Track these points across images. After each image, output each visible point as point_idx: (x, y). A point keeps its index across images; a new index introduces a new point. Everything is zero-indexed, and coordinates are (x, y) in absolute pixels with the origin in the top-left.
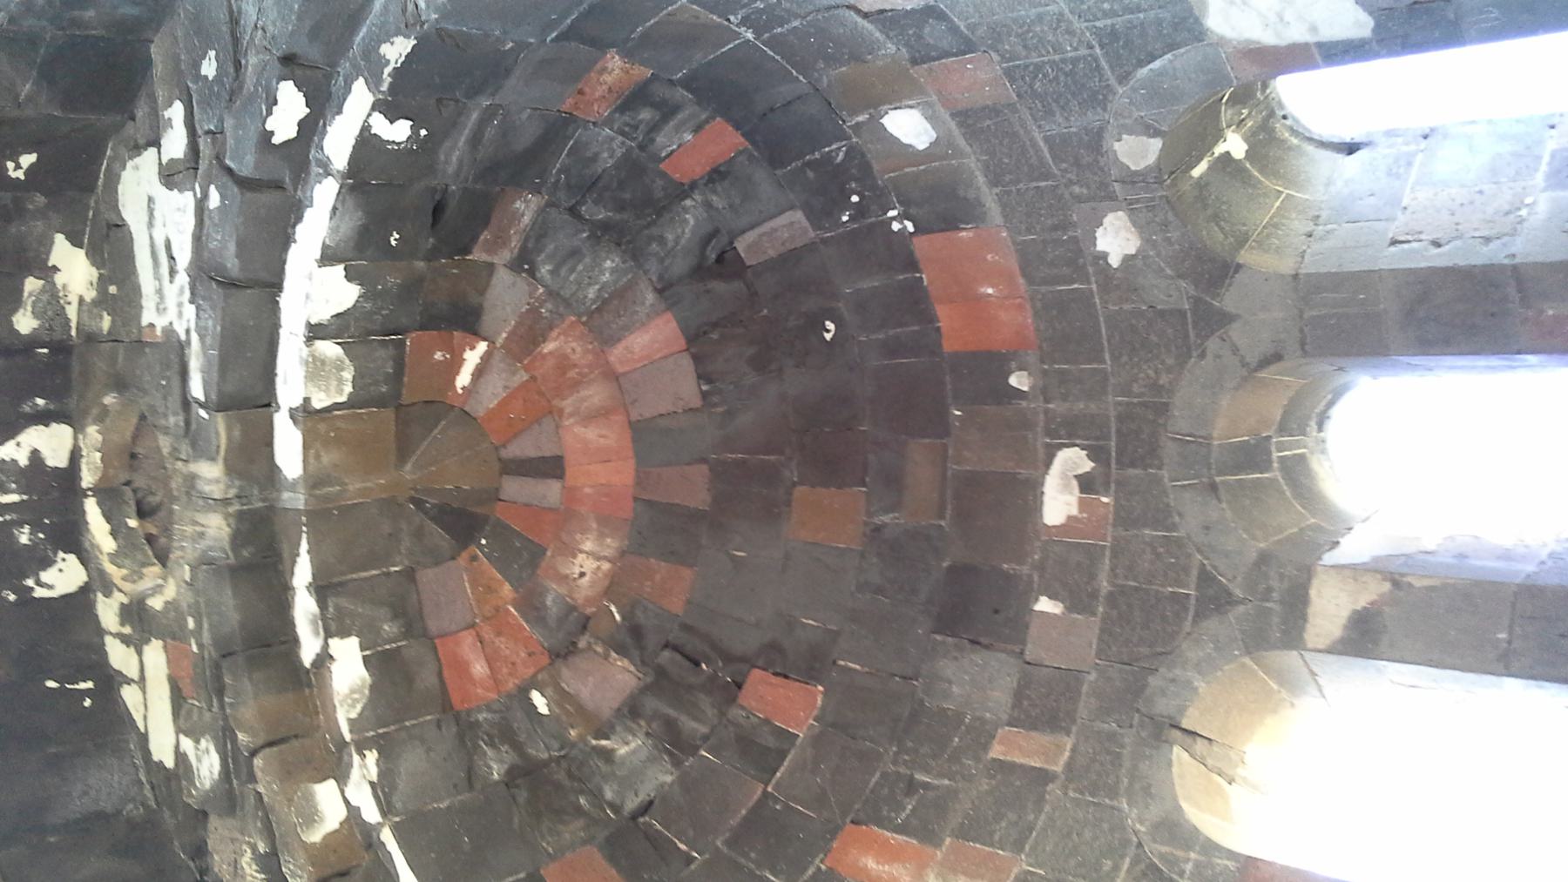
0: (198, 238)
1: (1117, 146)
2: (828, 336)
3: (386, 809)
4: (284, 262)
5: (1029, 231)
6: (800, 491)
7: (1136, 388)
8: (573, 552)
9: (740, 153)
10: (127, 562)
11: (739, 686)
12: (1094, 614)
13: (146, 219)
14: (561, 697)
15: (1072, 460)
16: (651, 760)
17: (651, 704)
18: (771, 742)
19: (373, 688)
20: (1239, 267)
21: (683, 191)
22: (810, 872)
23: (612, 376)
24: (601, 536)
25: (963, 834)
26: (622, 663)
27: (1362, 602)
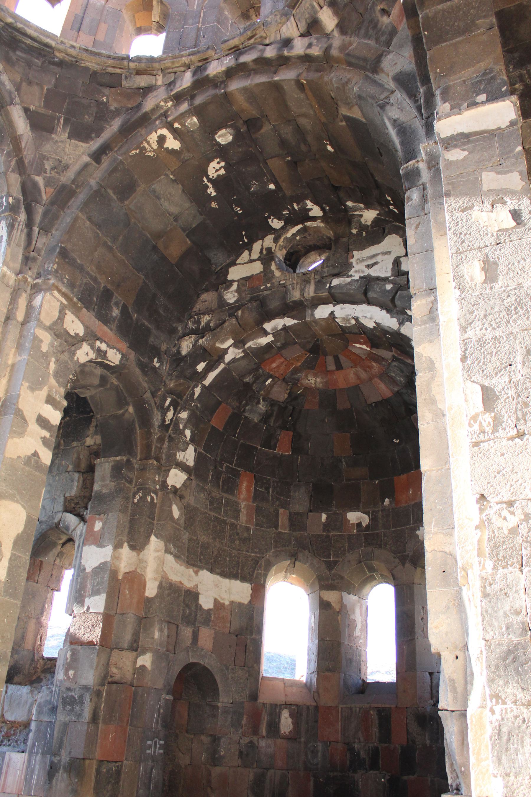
0: (378, 279)
2: (394, 440)
3: (229, 363)
4: (376, 305)
6: (349, 435)
7: (386, 538)
8: (315, 376)
10: (285, 243)
11: (287, 430)
12: (323, 532)
14: (271, 386)
15: (365, 520)
16: (260, 414)
17: (276, 408)
18: (272, 443)
22: (239, 469)
23: (370, 379)
24: (321, 382)
25: (258, 508)
26: (286, 396)
27: (333, 604)
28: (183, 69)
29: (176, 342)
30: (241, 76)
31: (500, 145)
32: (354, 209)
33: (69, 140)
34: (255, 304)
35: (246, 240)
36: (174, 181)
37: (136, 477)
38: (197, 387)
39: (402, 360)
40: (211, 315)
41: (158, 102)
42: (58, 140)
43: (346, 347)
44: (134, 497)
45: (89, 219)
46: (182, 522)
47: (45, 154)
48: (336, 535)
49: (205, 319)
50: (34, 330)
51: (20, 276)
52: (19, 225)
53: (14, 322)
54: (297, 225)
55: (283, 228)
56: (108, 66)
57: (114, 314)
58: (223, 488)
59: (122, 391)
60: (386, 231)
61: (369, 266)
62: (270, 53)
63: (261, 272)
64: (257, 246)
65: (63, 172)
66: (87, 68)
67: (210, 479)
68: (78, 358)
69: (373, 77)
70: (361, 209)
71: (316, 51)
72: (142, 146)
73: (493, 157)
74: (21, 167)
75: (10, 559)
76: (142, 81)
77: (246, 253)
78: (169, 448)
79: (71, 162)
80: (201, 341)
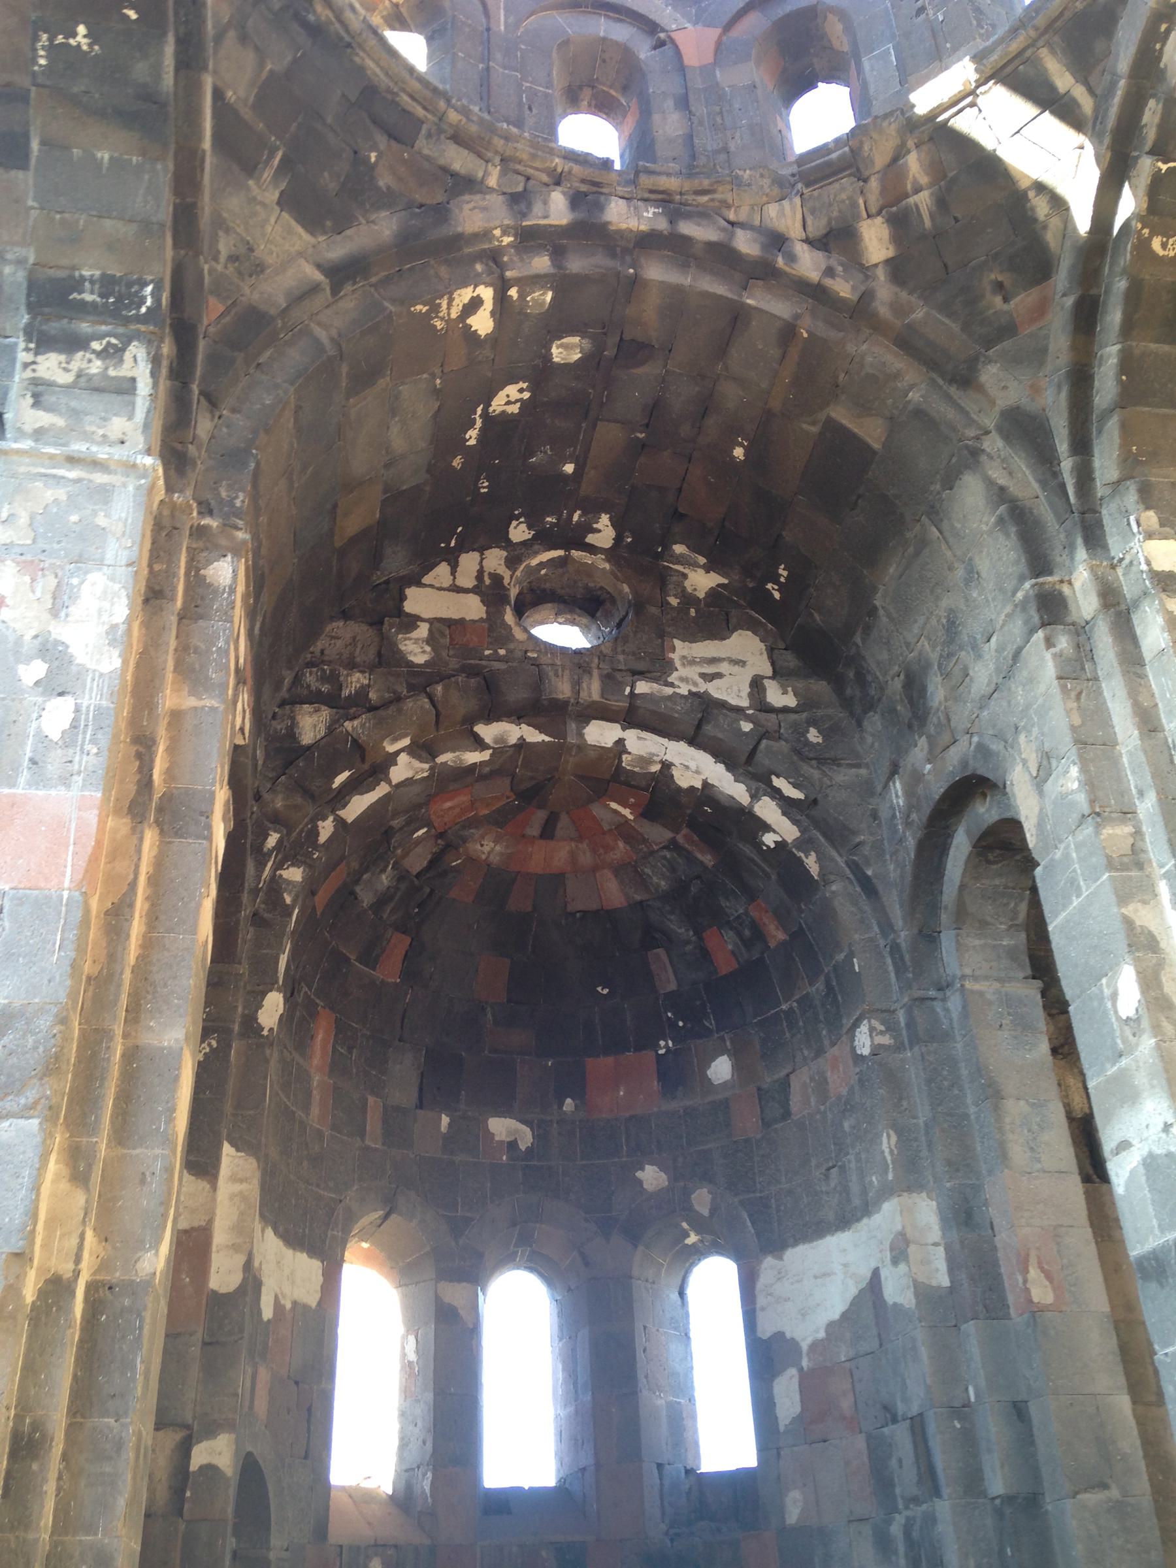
0: (723, 705)
1: (705, 1190)
2: (599, 989)
4: (705, 751)
8: (496, 842)
15: (526, 1137)
17: (403, 886)
20: (636, 1247)
21: (698, 932)
22: (318, 1001)
23: (595, 869)
24: (501, 854)
28: (545, 178)
30: (668, 256)
32: (680, 560)
33: (277, 209)
34: (473, 681)
36: (437, 392)
38: (324, 819)
39: (688, 851)
41: (492, 225)
43: (591, 801)
54: (556, 549)
56: (404, 90)
60: (733, 621)
61: (709, 678)
62: (746, 244)
63: (481, 620)
64: (469, 562)
65: (251, 276)
66: (362, 69)
70: (694, 565)
71: (843, 288)
76: (459, 160)
77: (443, 569)
79: (270, 261)
80: (348, 725)
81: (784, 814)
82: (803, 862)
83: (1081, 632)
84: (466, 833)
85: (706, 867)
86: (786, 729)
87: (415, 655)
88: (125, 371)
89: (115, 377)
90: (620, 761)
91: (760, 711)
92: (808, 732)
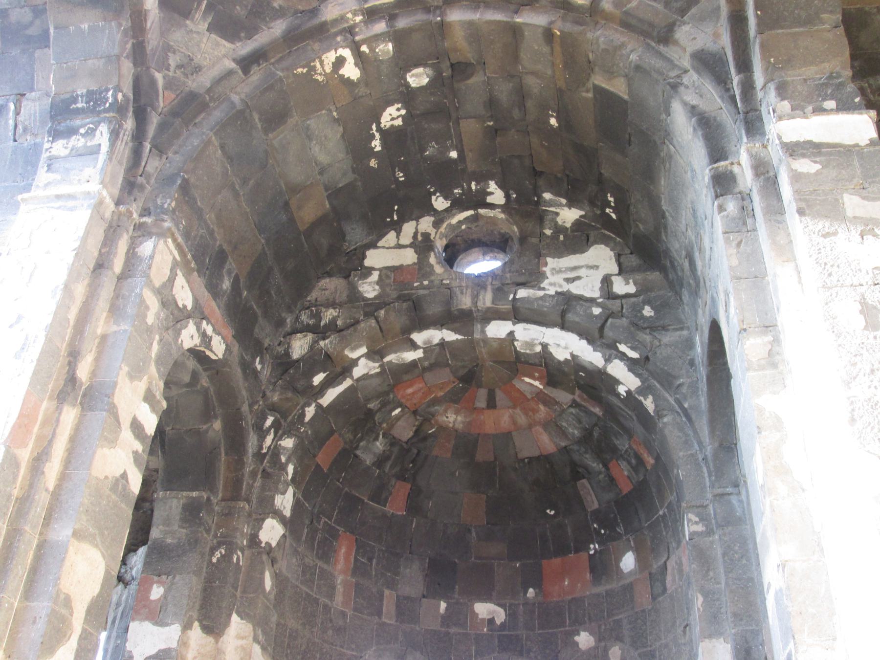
0: (580, 298)
1: (617, 647)
2: (548, 511)
3: (358, 380)
4: (572, 332)
5: (589, 604)
6: (484, 497)
8: (457, 413)
9: (620, 490)
10: (447, 230)
12: (441, 626)
13: (590, 264)
14: (398, 418)
15: (500, 615)
16: (375, 454)
17: (396, 450)
18: (383, 496)
19: (404, 364)
21: (606, 465)
22: (338, 528)
23: (530, 426)
24: (463, 423)
26: (411, 434)
29: (282, 339)
30: (466, 5)
31: (861, 165)
32: (550, 203)
34: (405, 305)
35: (395, 218)
36: (336, 121)
37: (217, 524)
38: (309, 405)
39: (584, 407)
40: (337, 310)
41: (344, 11)
42: (194, 30)
43: (511, 379)
44: (212, 554)
45: (222, 147)
46: (272, 597)
47: (172, 44)
48: (459, 634)
49: (329, 314)
50: (141, 290)
51: (122, 208)
52: (124, 135)
53: (110, 272)
55: (446, 210)
57: (224, 287)
58: (317, 553)
59: (212, 396)
60: (591, 239)
61: (569, 280)
63: (414, 264)
64: (409, 228)
65: (192, 74)
67: (304, 538)
68: (182, 341)
69: (656, 48)
70: (560, 205)
72: (312, 64)
73: (854, 178)
74: (139, 54)
75: (80, 636)
78: (263, 488)
79: (205, 64)
80: (322, 343)
81: (630, 370)
82: (642, 403)
83: (745, 198)
84: (432, 409)
85: (599, 417)
86: (627, 309)
87: (369, 292)
88: (95, 142)
89: (91, 146)
90: (515, 348)
91: (609, 298)
92: (643, 309)
